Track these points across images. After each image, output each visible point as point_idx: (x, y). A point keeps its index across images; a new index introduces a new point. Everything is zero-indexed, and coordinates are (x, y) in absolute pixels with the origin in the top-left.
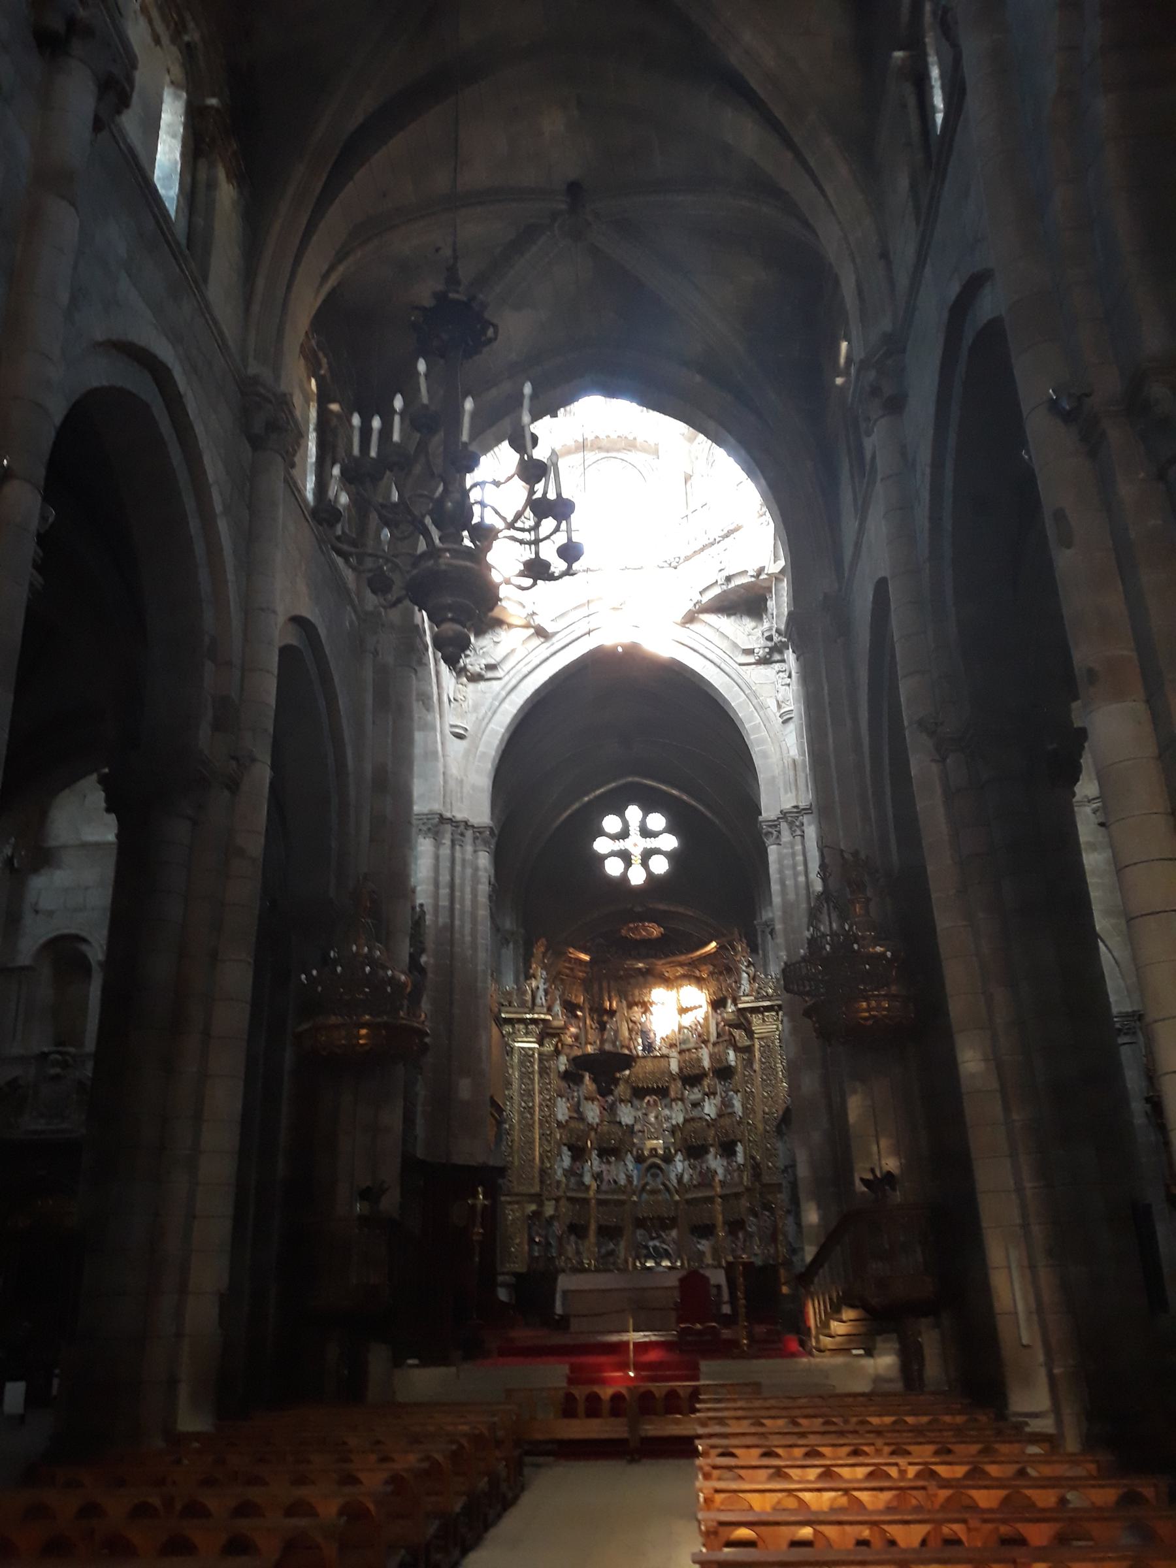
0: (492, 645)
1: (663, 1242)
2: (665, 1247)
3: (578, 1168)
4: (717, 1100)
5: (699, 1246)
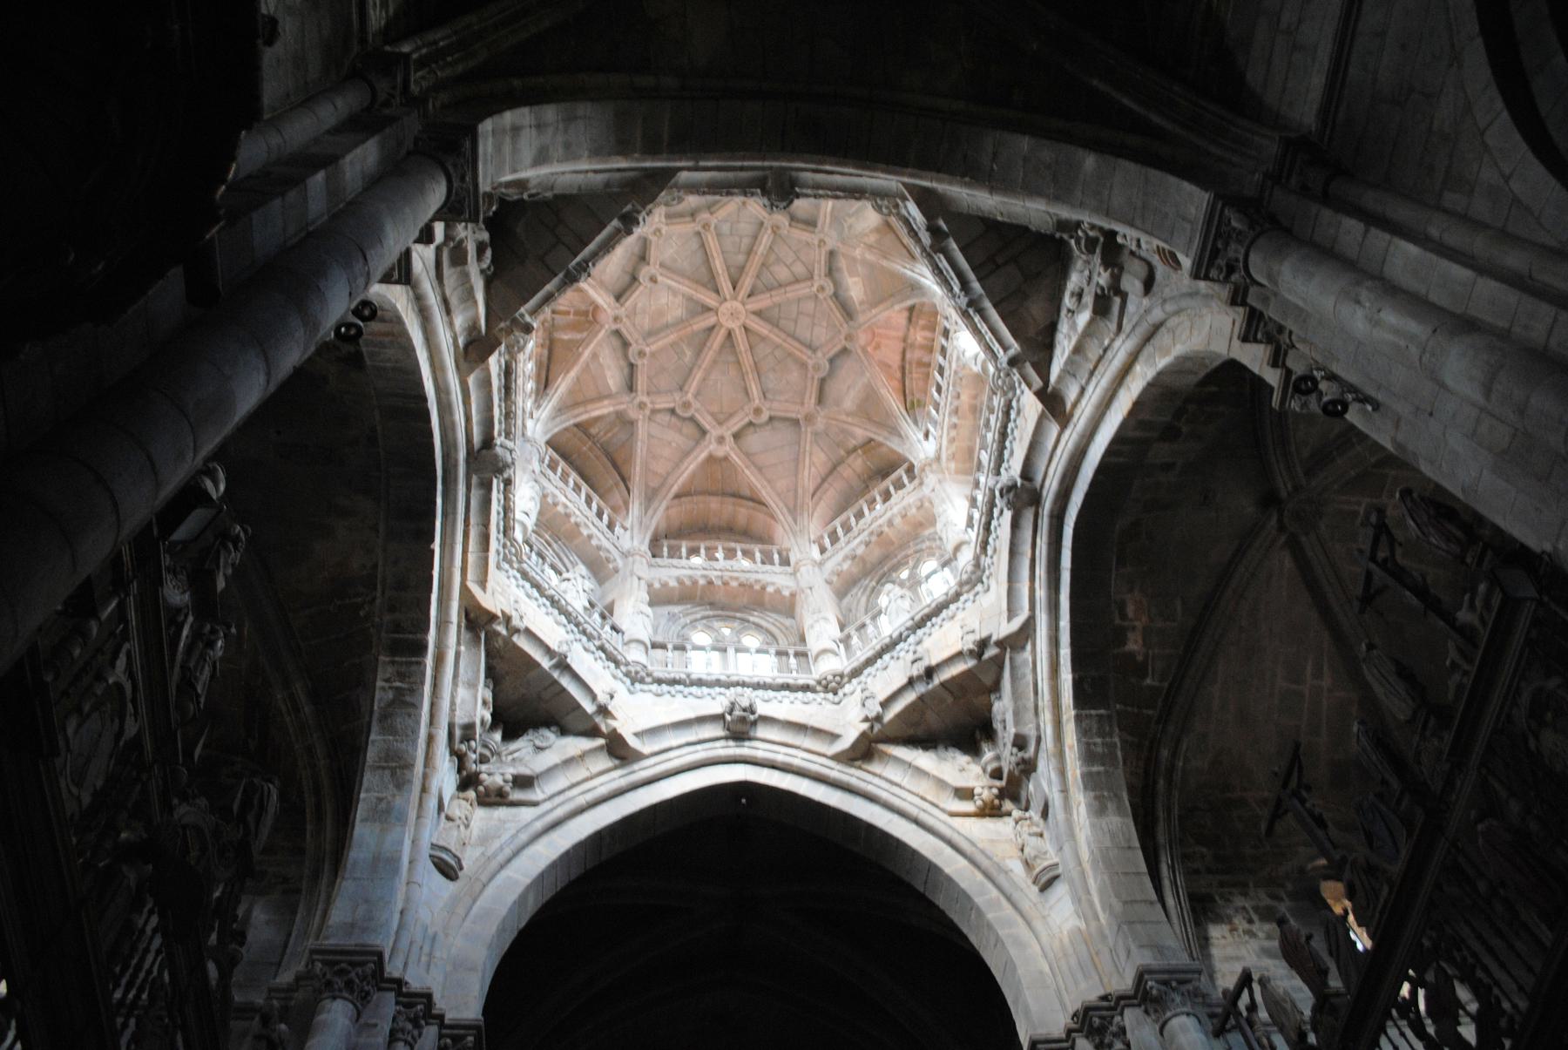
0: (530, 749)
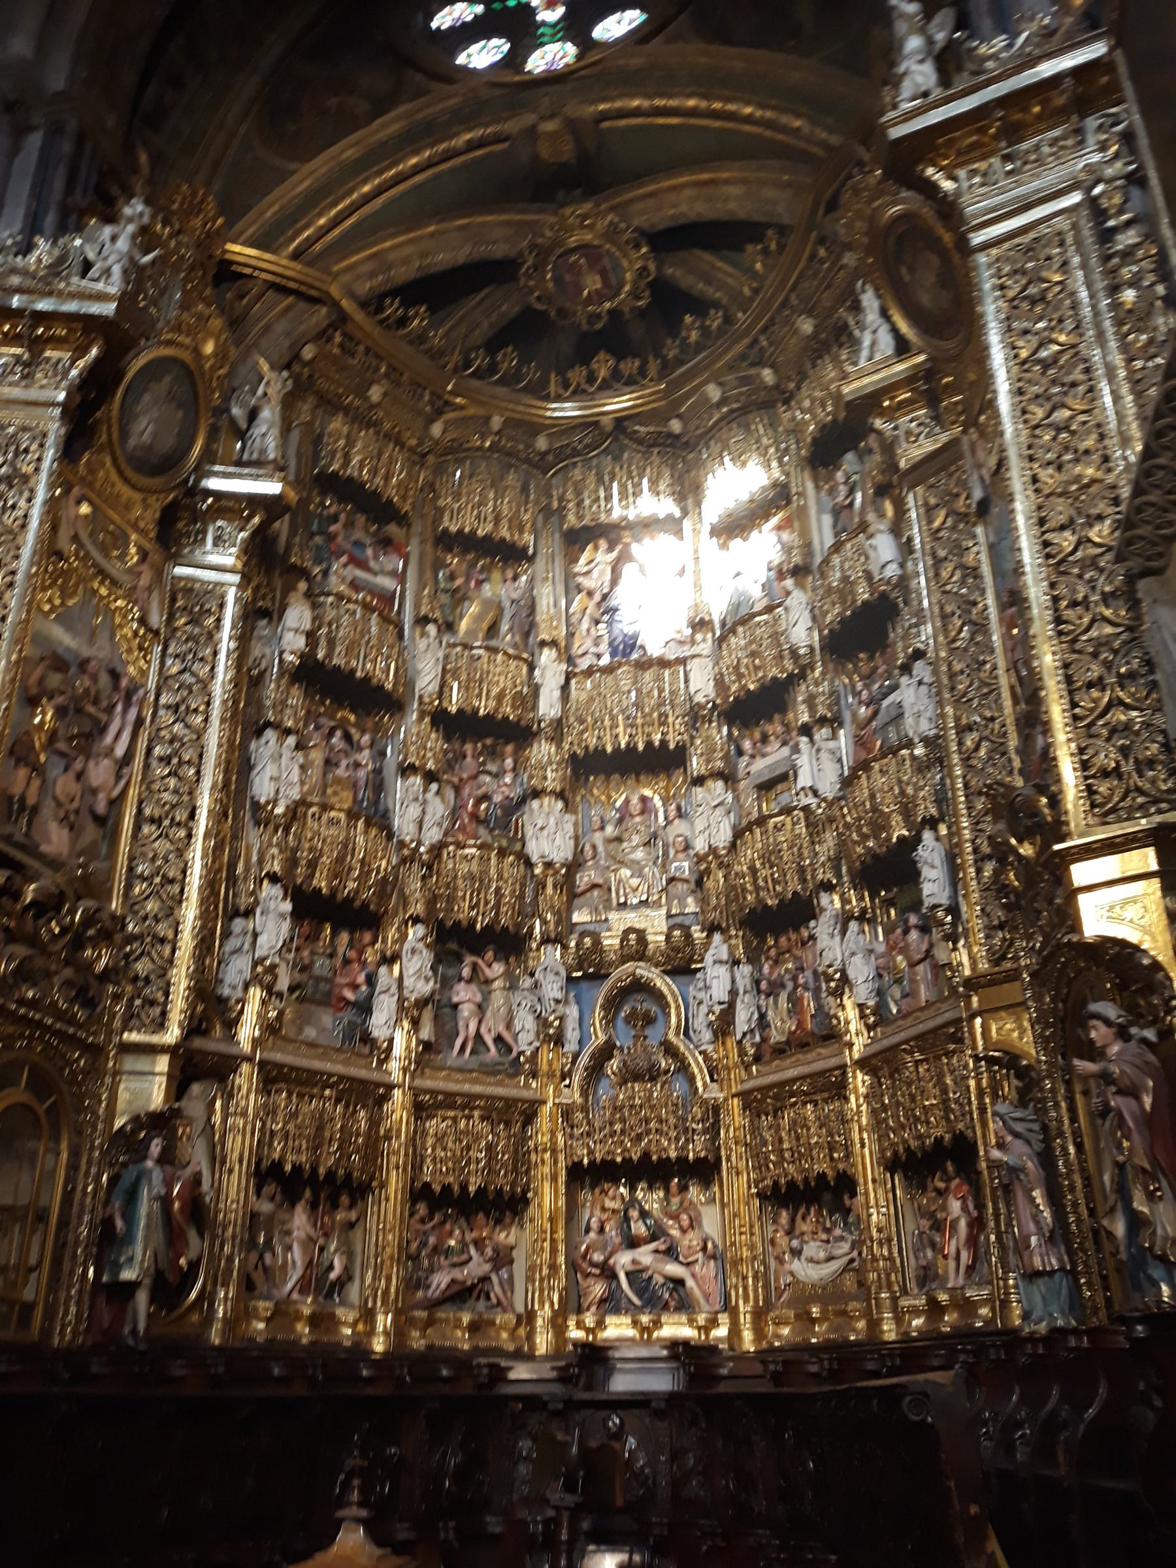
1: (671, 1253)
2: (673, 1269)
3: (355, 987)
4: (844, 739)
5: (797, 1266)
